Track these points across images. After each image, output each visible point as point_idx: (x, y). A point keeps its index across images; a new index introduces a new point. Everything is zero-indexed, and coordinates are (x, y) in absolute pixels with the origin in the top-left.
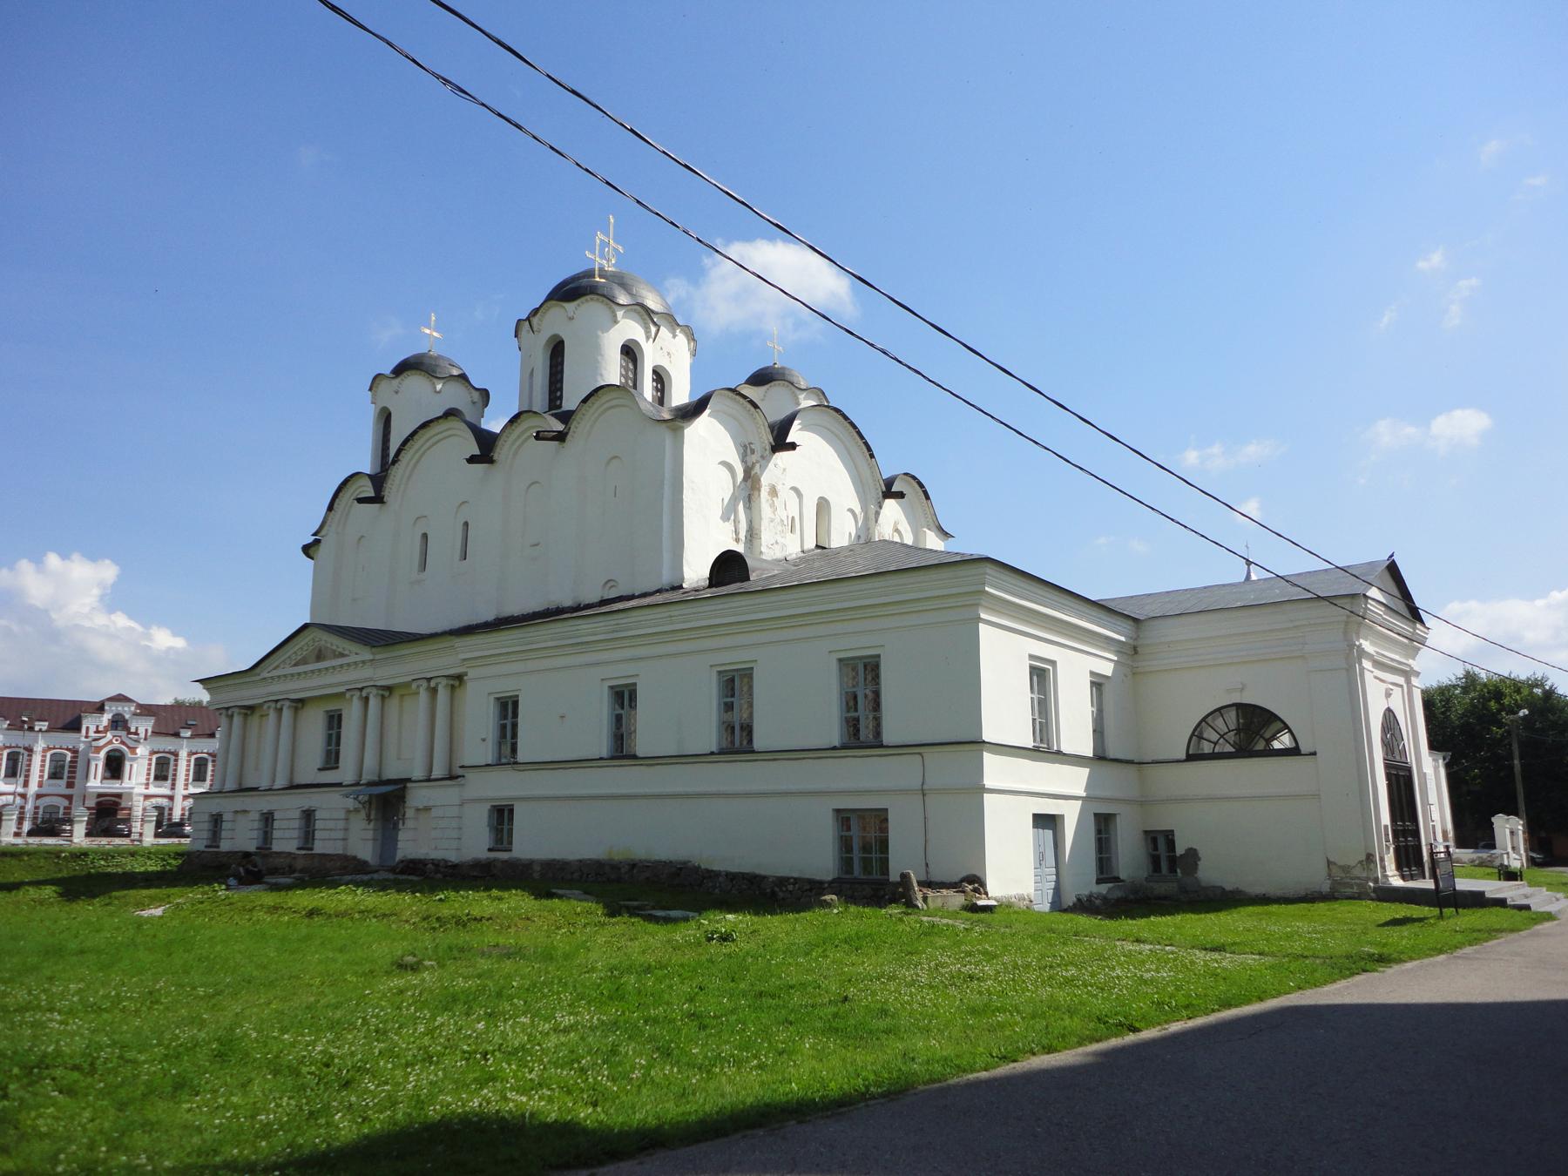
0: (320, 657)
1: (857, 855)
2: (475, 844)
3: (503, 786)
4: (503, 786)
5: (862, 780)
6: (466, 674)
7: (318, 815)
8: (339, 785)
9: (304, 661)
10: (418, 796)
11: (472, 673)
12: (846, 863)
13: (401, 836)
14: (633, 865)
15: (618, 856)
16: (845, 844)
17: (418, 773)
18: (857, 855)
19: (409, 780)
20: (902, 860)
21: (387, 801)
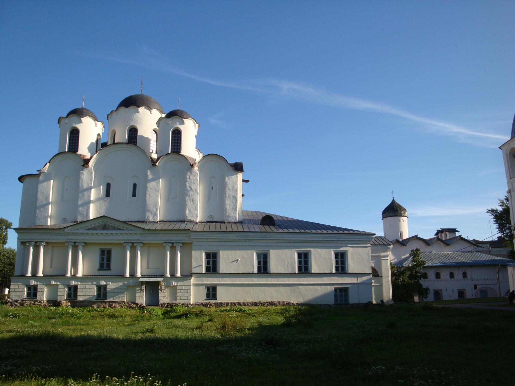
0: (104, 228)
1: (339, 298)
3: (212, 281)
4: (212, 281)
6: (192, 243)
7: (108, 287)
9: (94, 229)
11: (194, 243)
12: (336, 300)
13: (160, 295)
16: (336, 296)
18: (339, 298)
20: (353, 299)
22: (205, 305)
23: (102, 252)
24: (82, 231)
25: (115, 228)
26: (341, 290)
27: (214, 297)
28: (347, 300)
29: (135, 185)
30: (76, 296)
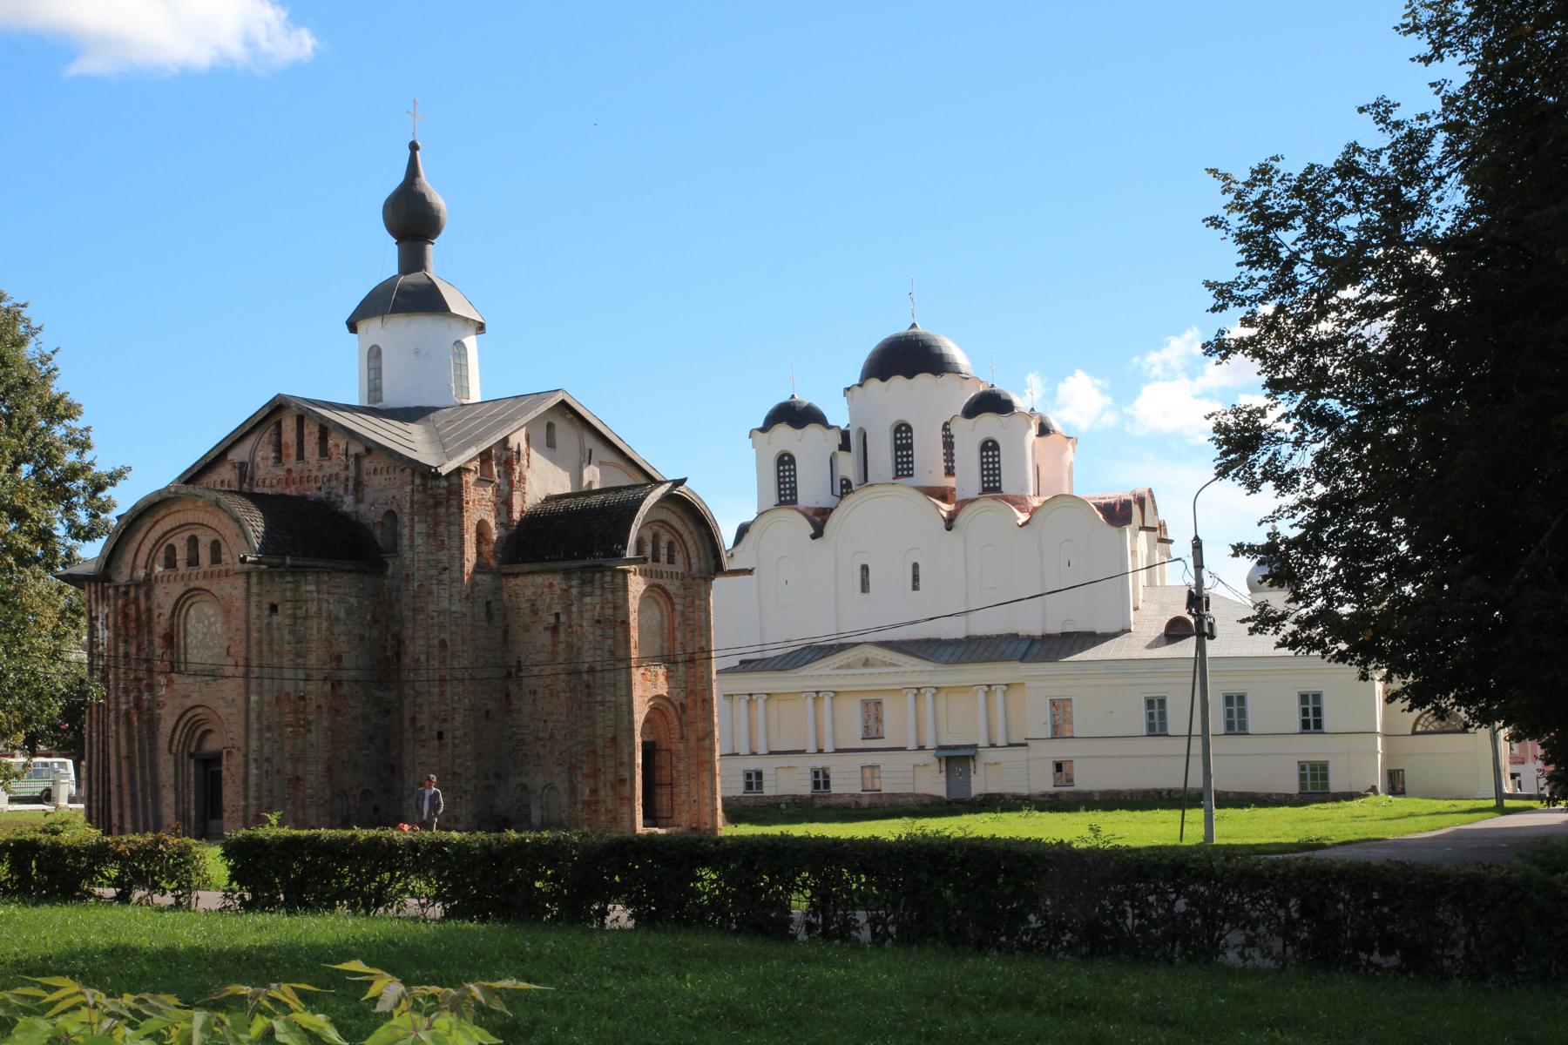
1: (1309, 782)
2: (1044, 783)
3: (1061, 750)
4: (1061, 750)
5: (1313, 748)
8: (903, 749)
9: (849, 666)
10: (987, 756)
12: (1303, 786)
14: (1170, 791)
15: (1159, 786)
16: (1302, 777)
17: (983, 742)
18: (1309, 782)
19: (975, 747)
20: (1335, 785)
21: (957, 760)
22: (1056, 796)
23: (866, 704)
24: (829, 671)
25: (885, 664)
26: (1314, 766)
27: (1070, 781)
28: (1326, 786)
29: (916, 566)
30: (827, 784)
